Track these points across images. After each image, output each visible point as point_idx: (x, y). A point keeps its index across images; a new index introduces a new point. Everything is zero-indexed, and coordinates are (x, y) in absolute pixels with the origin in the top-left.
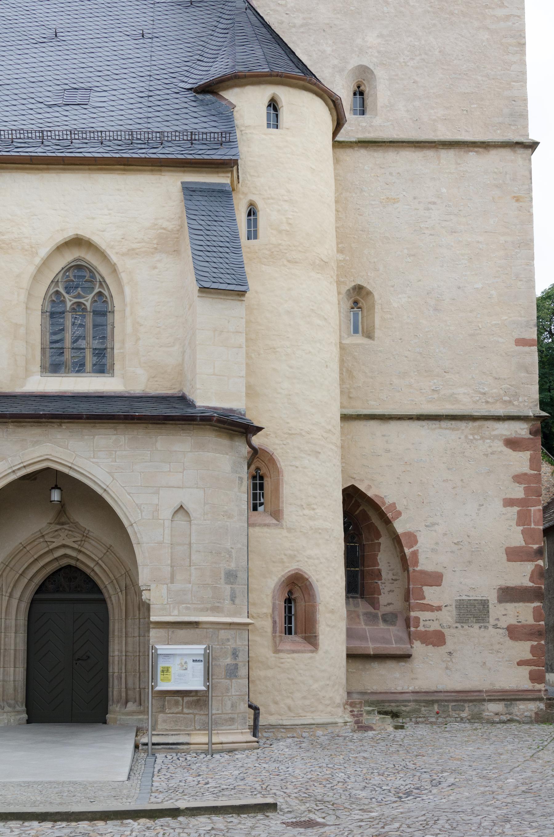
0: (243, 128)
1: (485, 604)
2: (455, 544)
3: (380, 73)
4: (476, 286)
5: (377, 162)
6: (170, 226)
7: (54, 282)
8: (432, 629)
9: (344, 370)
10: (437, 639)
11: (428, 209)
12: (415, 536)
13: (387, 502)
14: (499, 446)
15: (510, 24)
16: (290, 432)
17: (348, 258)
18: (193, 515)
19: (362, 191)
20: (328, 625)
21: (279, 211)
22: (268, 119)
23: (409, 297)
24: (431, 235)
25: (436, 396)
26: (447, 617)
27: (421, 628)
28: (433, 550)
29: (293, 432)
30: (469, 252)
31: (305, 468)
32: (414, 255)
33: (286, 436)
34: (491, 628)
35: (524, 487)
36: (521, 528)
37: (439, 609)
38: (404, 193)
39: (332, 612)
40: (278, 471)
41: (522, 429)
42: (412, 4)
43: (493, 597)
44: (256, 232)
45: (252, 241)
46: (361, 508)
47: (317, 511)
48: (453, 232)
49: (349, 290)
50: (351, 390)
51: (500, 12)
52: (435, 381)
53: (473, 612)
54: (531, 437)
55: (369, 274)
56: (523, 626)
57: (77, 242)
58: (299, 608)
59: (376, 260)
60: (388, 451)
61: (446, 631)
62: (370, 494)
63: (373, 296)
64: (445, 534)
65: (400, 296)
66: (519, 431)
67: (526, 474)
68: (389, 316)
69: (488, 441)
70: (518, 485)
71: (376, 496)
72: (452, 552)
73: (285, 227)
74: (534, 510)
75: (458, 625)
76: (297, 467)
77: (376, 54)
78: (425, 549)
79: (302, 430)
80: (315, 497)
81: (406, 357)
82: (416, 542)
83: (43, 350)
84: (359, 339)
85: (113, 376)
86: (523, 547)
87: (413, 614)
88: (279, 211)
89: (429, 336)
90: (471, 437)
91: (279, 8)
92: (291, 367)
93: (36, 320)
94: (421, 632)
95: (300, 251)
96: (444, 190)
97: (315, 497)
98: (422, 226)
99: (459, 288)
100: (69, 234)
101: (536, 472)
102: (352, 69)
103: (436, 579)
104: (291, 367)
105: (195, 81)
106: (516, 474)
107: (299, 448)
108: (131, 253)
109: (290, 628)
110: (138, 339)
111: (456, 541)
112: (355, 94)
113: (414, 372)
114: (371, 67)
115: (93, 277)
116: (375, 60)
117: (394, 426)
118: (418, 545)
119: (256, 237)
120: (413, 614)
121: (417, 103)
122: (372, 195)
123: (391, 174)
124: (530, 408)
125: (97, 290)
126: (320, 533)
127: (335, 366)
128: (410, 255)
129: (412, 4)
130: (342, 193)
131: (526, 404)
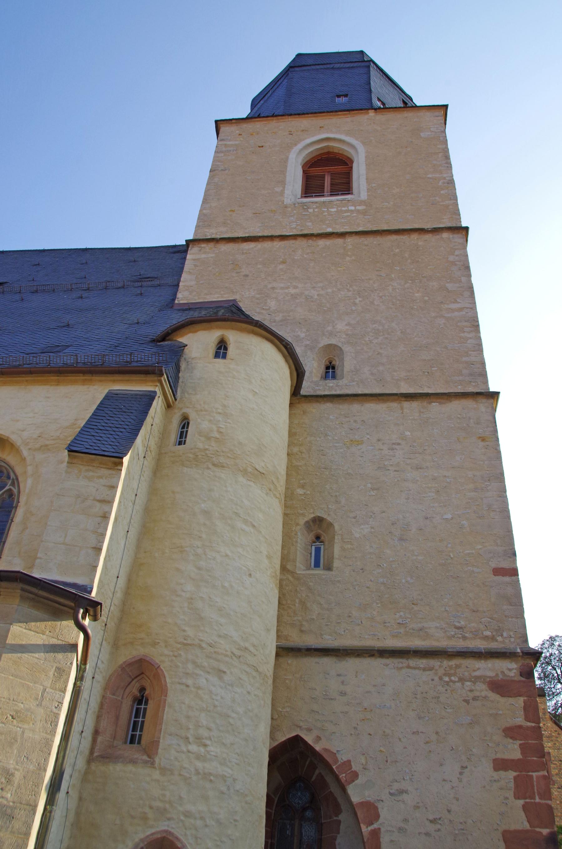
0: (189, 360)
2: (431, 821)
3: (346, 349)
4: (445, 517)
5: (342, 413)
9: (297, 601)
11: (392, 449)
12: (376, 808)
13: (339, 759)
14: (482, 689)
16: (185, 642)
17: (309, 492)
19: (326, 435)
23: (372, 528)
24: (395, 471)
25: (402, 630)
28: (401, 830)
29: (189, 642)
30: (436, 485)
31: (199, 688)
32: (377, 489)
33: (179, 646)
35: (520, 745)
36: (522, 802)
38: (368, 436)
40: (164, 691)
41: (510, 670)
46: (317, 772)
47: (209, 748)
49: (307, 522)
50: (304, 623)
52: (402, 614)
54: (523, 679)
55: (330, 507)
59: (337, 494)
60: (343, 694)
62: (318, 748)
63: (334, 527)
64: (417, 807)
65: (362, 526)
66: (507, 672)
67: (520, 727)
68: (349, 546)
69: (468, 683)
70: (511, 741)
71: (326, 750)
72: (427, 834)
74: (537, 776)
76: (188, 686)
77: (344, 336)
78: (389, 828)
79: (201, 640)
80: (210, 729)
81: (368, 587)
82: (377, 817)
86: (527, 831)
88: (210, 421)
89: (394, 566)
90: (446, 679)
92: (199, 569)
95: (228, 457)
96: (408, 433)
97: (210, 729)
98: (386, 463)
99: (427, 518)
101: (533, 725)
102: (323, 347)
104: (199, 569)
106: (508, 726)
111: (431, 818)
113: (377, 603)
114: (340, 345)
117: (351, 665)
118: (381, 820)
121: (381, 368)
122: (336, 438)
123: (355, 421)
124: (518, 644)
126: (211, 781)
128: (373, 489)
130: (306, 438)
131: (512, 640)
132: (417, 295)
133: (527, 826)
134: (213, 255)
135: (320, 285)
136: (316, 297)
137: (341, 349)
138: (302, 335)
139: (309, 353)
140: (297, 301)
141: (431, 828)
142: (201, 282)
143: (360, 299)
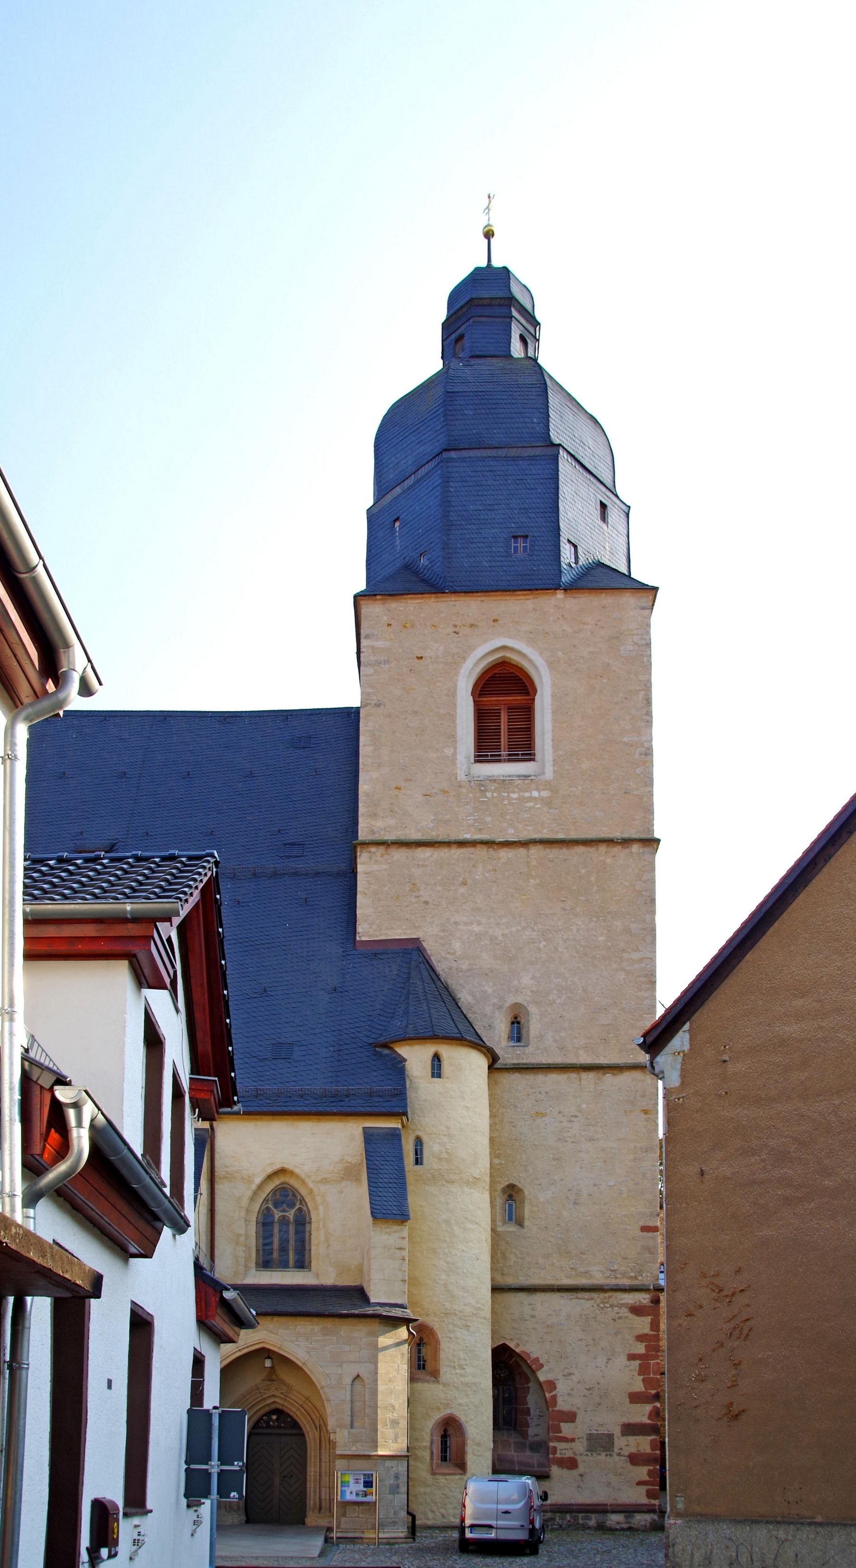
1: (610, 1437)
3: (532, 1009)
6: (354, 1161)
7: (266, 1200)
8: (567, 1456)
10: (571, 1464)
11: (571, 1121)
15: (643, 965)
18: (366, 1381)
20: (474, 1454)
21: (439, 1143)
22: (433, 1068)
25: (573, 1273)
26: (580, 1447)
27: (558, 1455)
28: (569, 1394)
32: (558, 1159)
34: (615, 1456)
36: (642, 1377)
37: (573, 1440)
39: (479, 1445)
42: (560, 950)
43: (617, 1431)
44: (422, 1158)
45: (419, 1167)
48: (591, 1139)
51: (636, 956)
53: (601, 1443)
56: (642, 1454)
57: (282, 1171)
58: (452, 1442)
60: (533, 1316)
61: (578, 1458)
64: (579, 1382)
72: (585, 1396)
73: (445, 1155)
75: (589, 1454)
82: (555, 1388)
83: (257, 1251)
84: (512, 1228)
85: (310, 1270)
87: (551, 1444)
91: (449, 956)
93: (253, 1229)
94: (558, 1458)
96: (584, 1106)
100: (277, 1166)
103: (571, 1417)
105: (375, 1036)
107: (453, 1324)
108: (325, 1181)
109: (446, 1457)
110: (329, 1246)
112: (513, 1023)
114: (525, 1004)
115: (294, 1195)
116: (528, 998)
117: (538, 1297)
119: (421, 1164)
120: (551, 1444)
121: (563, 1034)
125: (298, 1206)
127: (486, 1258)
128: (554, 1159)
129: (560, 950)
132: (600, 938)
133: (643, 1389)
134: (386, 867)
135: (504, 920)
136: (500, 938)
137: (526, 1009)
138: (490, 991)
139: (497, 1013)
140: (482, 943)
141: (587, 1393)
142: (380, 909)
143: (544, 943)
